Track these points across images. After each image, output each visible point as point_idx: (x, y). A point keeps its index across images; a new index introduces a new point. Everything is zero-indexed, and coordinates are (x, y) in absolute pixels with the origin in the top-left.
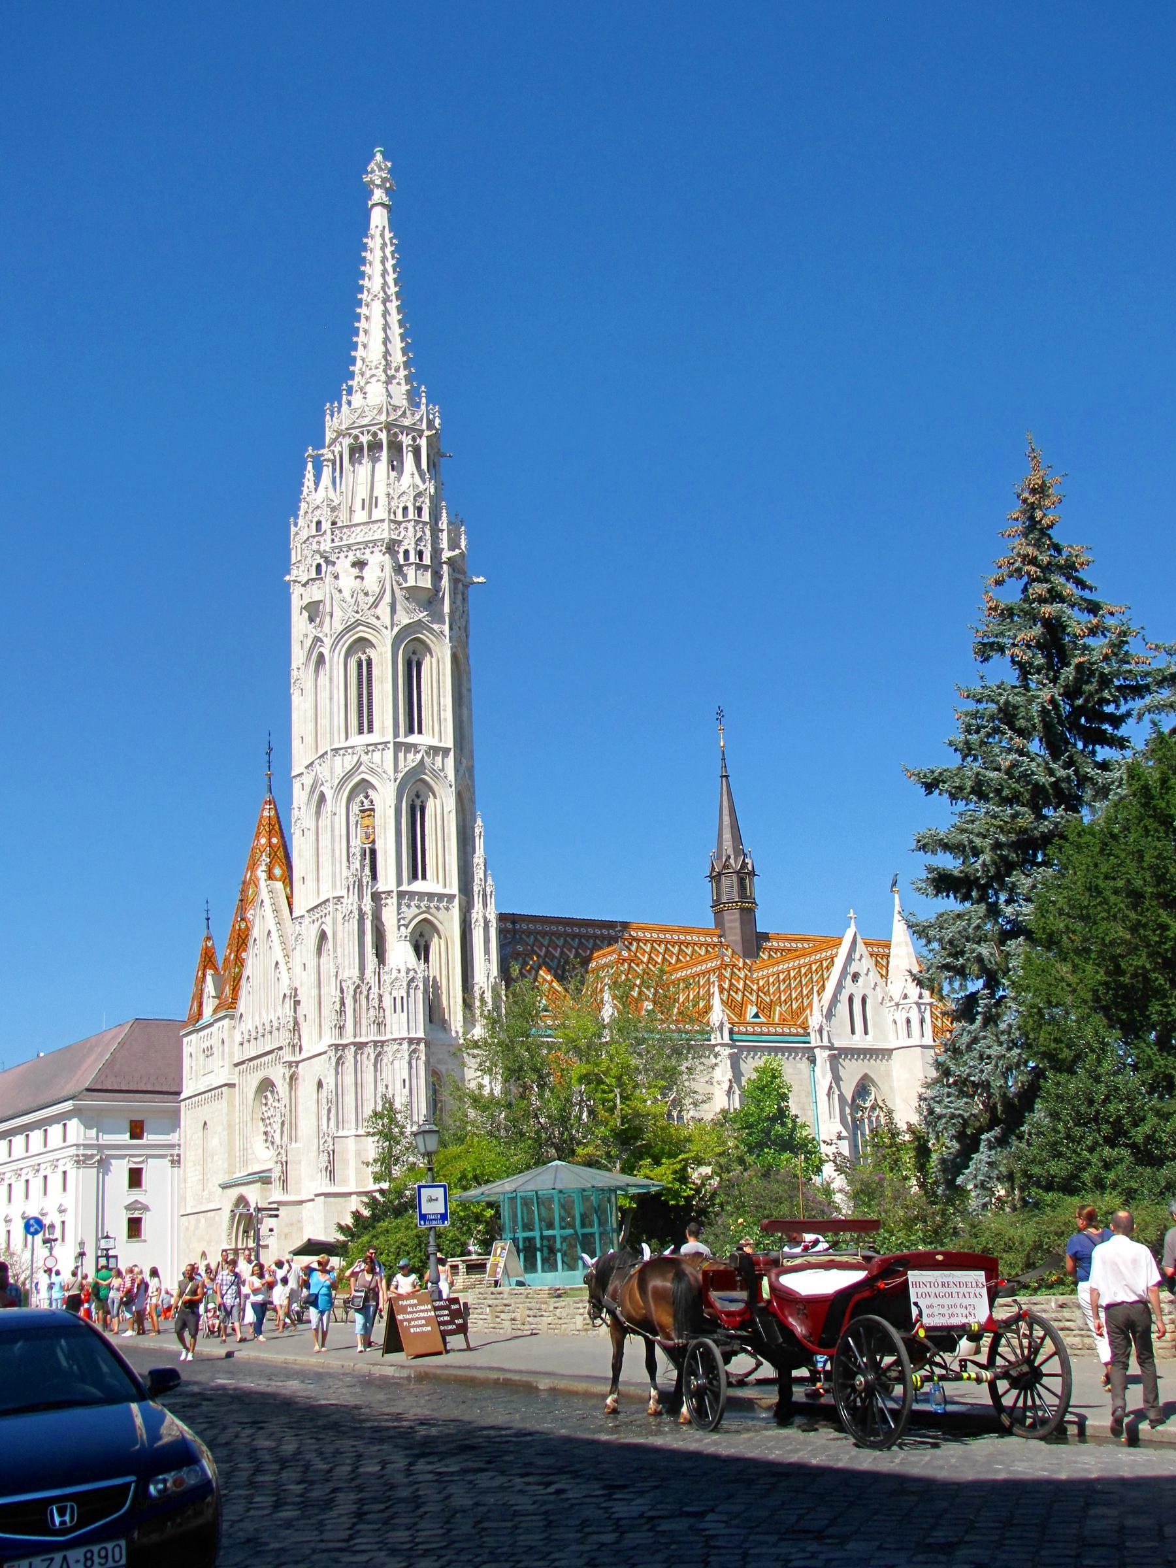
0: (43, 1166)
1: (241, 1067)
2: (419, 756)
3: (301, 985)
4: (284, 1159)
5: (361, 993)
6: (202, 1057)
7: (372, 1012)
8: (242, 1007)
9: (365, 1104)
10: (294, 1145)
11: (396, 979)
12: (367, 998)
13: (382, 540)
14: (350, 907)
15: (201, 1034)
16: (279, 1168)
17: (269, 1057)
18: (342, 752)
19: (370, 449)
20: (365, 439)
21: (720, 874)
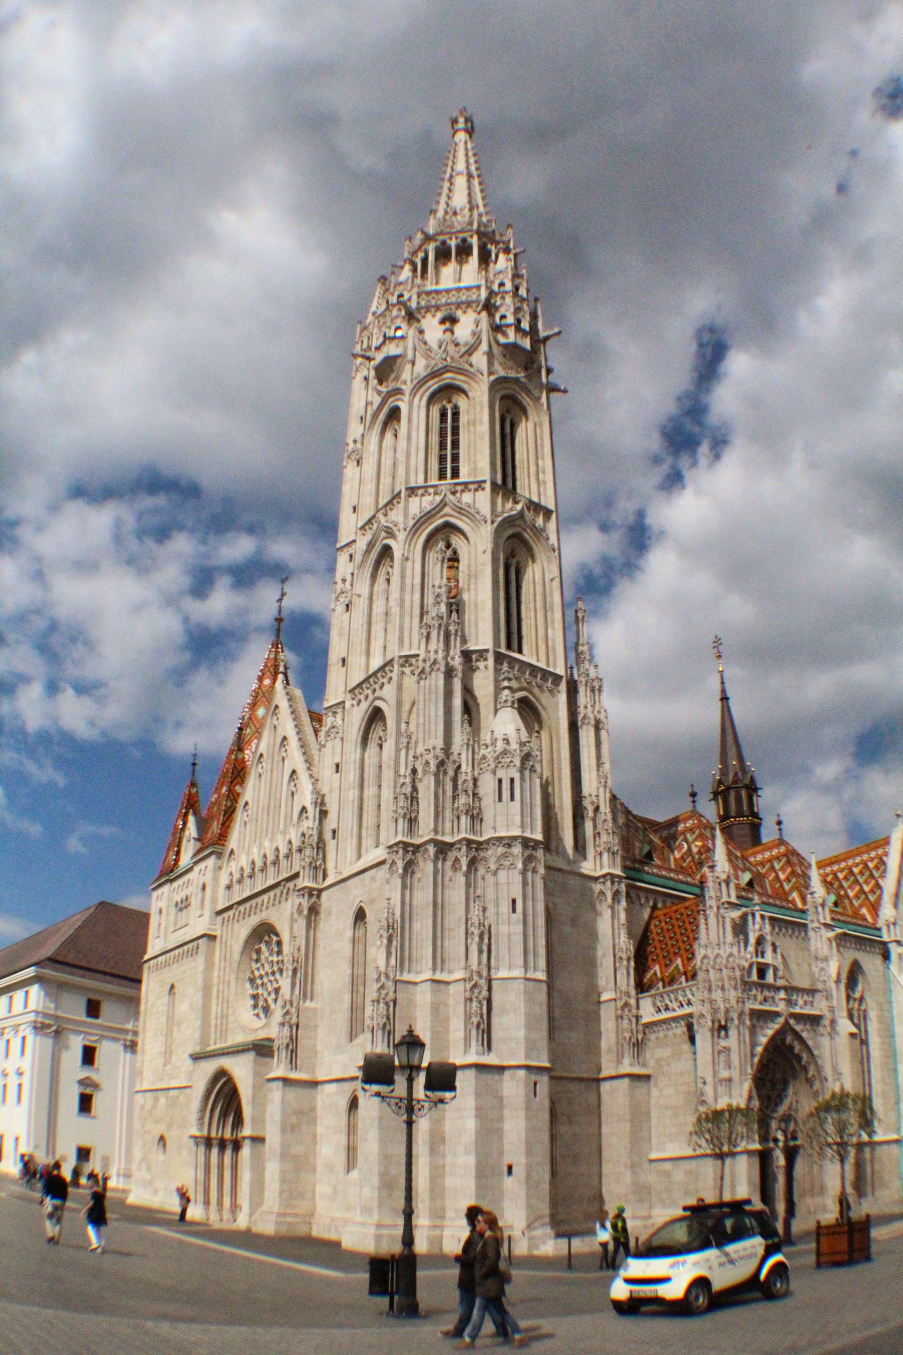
0: (6, 1031)
1: (226, 915)
2: (519, 507)
3: (331, 791)
4: (294, 1020)
5: (445, 773)
6: (173, 910)
7: (462, 800)
8: (233, 842)
9: (446, 933)
10: (308, 1004)
11: (505, 752)
12: (455, 780)
13: (478, 302)
14: (432, 656)
15: (176, 884)
16: (286, 1031)
17: (272, 894)
18: (420, 492)
19: (457, 255)
20: (453, 243)
21: (728, 789)
